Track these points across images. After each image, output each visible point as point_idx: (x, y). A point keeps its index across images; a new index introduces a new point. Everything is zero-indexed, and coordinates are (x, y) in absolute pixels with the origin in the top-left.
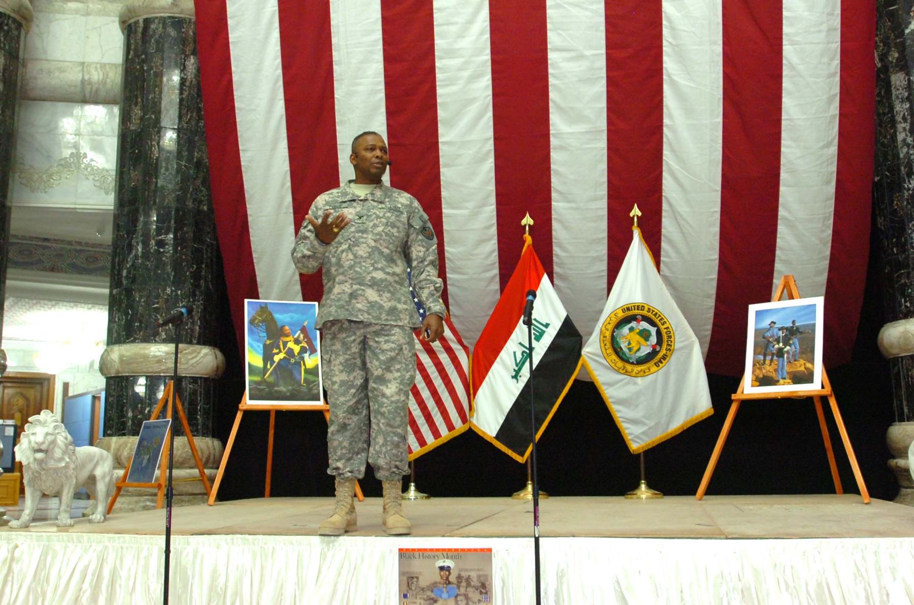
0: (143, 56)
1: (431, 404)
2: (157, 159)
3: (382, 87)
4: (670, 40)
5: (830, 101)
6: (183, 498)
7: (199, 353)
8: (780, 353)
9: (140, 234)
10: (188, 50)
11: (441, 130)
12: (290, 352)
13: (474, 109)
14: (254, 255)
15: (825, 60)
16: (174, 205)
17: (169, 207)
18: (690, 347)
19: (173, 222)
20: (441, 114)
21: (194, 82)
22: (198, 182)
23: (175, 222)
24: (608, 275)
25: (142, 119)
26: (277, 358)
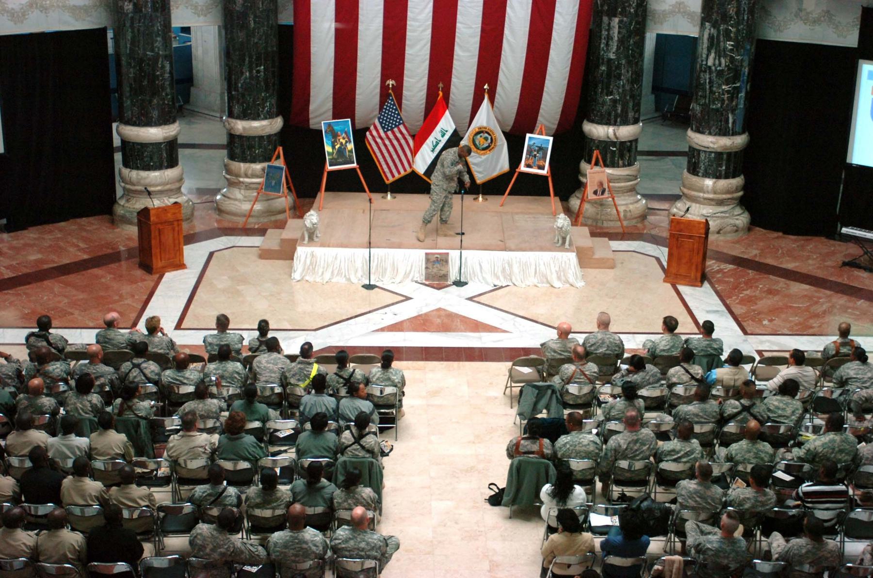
1: (397, 161)
8: (535, 156)
11: (407, 48)
12: (341, 143)
13: (423, 43)
18: (503, 145)
20: (408, 42)
24: (473, 108)
25: (243, 5)
26: (337, 147)
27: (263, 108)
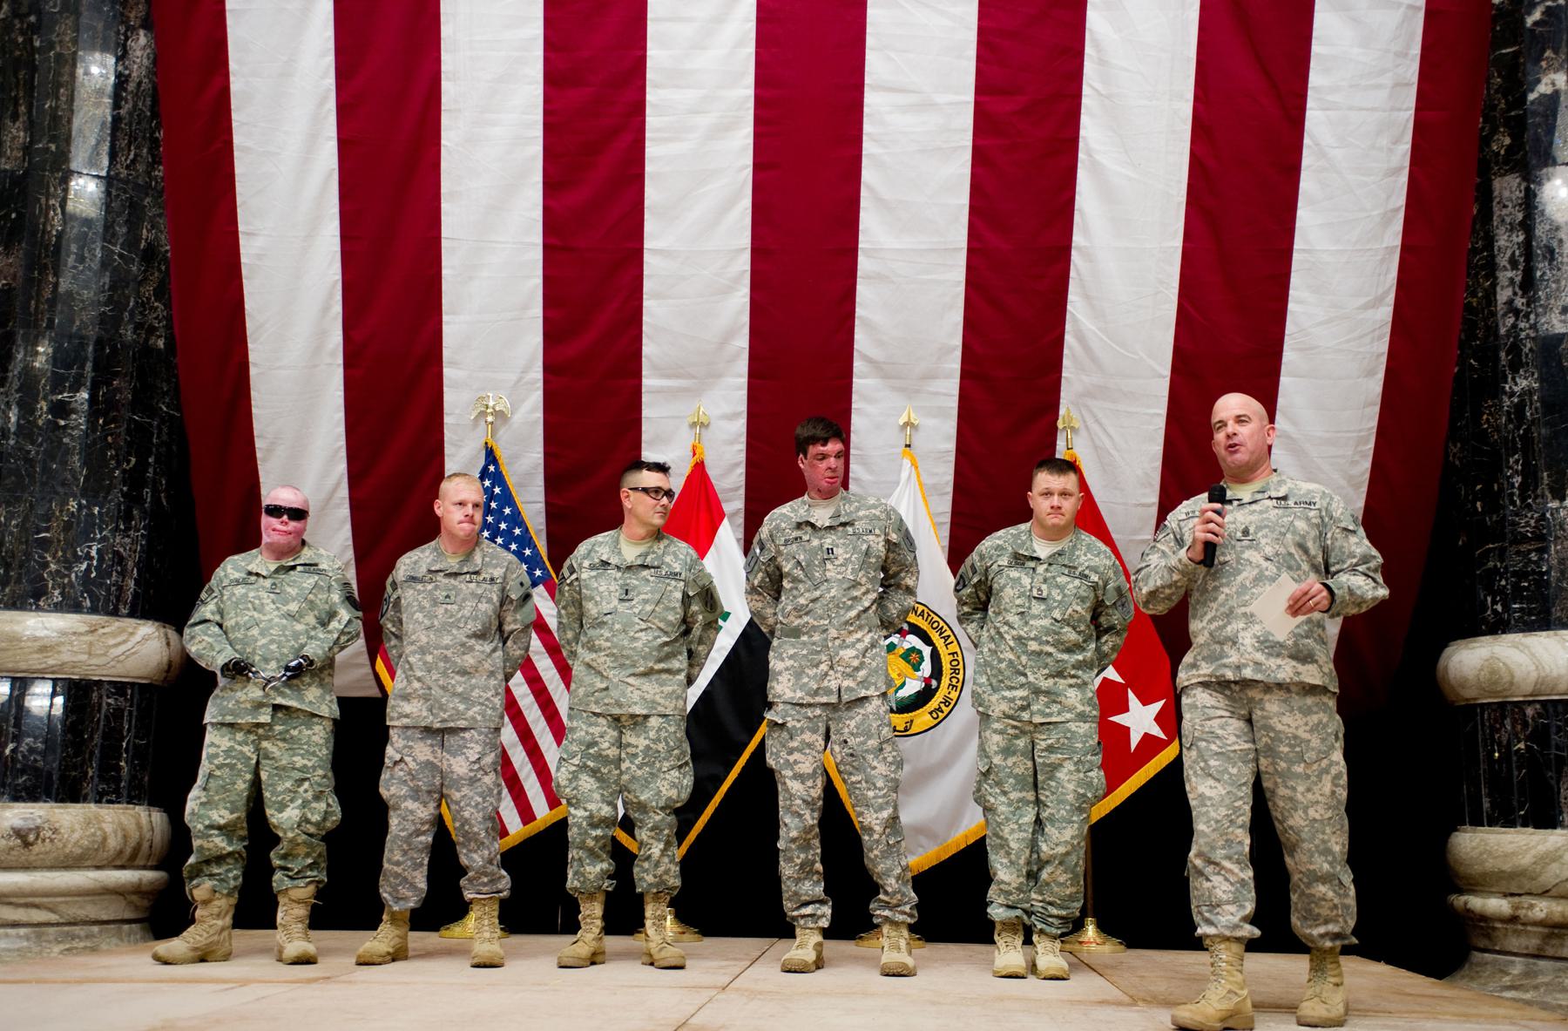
0: (32, 19)
2: (60, 235)
3: (538, 132)
4: (1096, 85)
5: (1386, 220)
6: (76, 929)
7: (132, 634)
9: (16, 384)
10: (134, 16)
14: (259, 444)
15: (1384, 141)
16: (92, 333)
17: (82, 337)
19: (89, 366)
21: (146, 84)
22: (148, 290)
23: (95, 369)
25: (27, 149)
27: (68, 564)
